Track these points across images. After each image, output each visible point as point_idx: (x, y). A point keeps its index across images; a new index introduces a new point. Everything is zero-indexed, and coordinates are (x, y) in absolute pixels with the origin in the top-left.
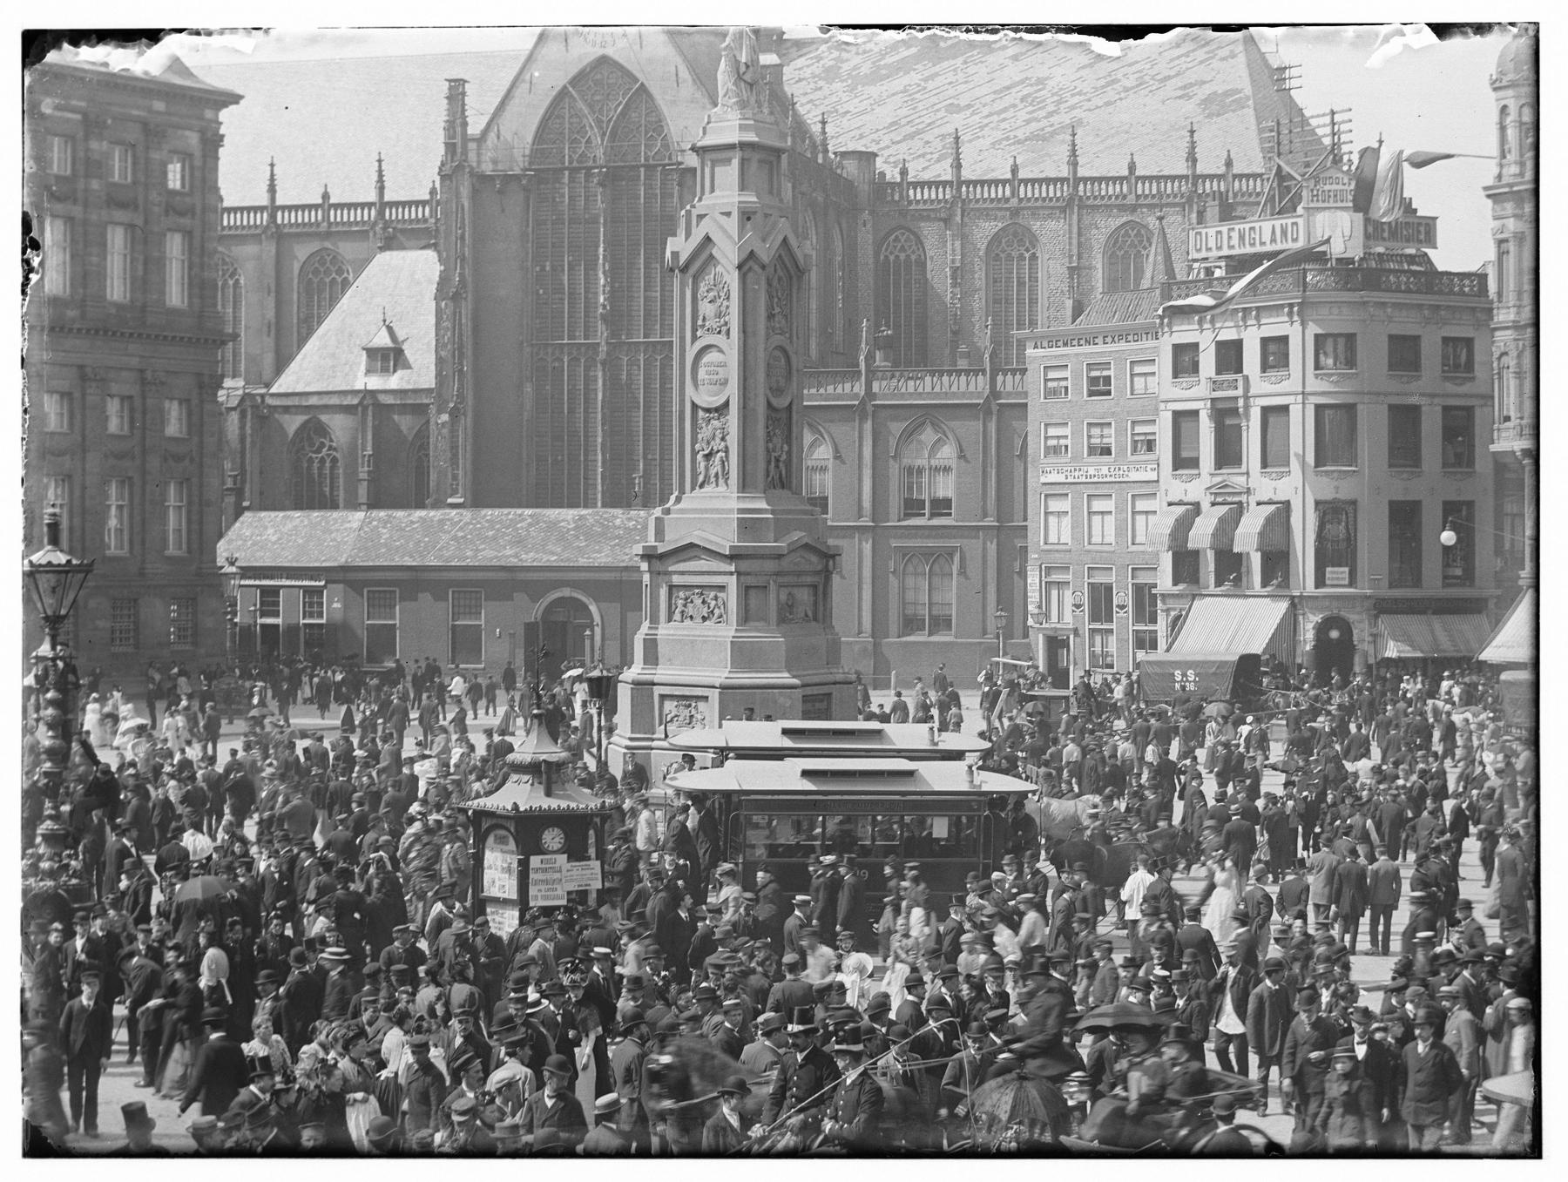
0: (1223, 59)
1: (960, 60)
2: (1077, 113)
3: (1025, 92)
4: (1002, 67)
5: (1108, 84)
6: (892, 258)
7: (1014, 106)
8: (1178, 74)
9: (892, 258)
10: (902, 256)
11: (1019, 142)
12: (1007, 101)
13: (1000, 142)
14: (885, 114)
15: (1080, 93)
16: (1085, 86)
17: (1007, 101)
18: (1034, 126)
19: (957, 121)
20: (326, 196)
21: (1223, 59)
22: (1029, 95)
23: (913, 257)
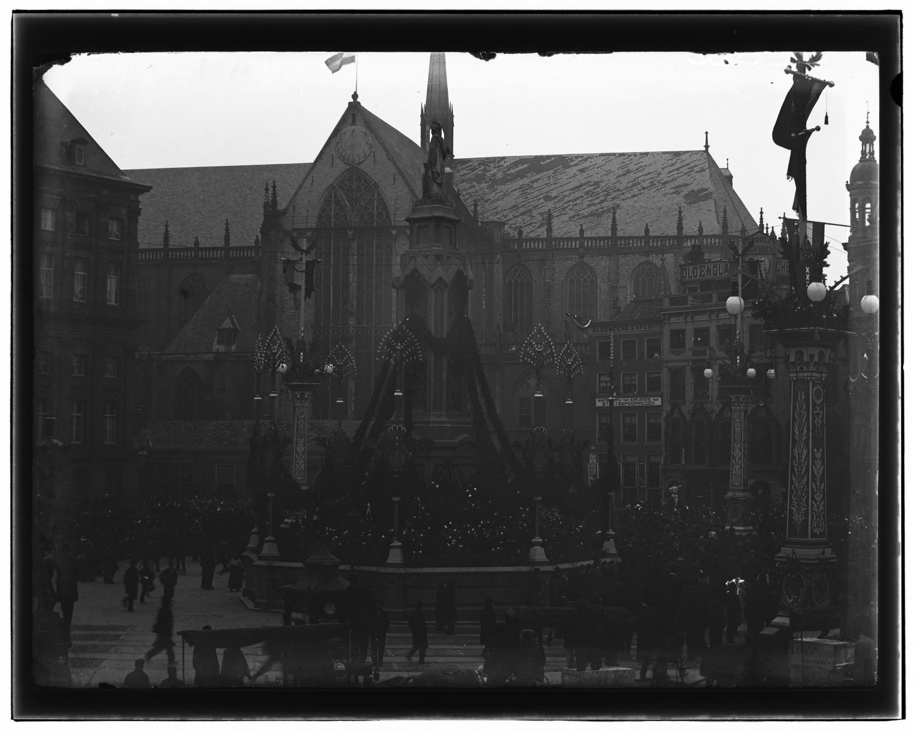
0: (696, 172)
1: (552, 171)
2: (618, 201)
3: (587, 190)
5: (635, 185)
6: (513, 281)
7: (582, 197)
9: (513, 281)
10: (519, 280)
11: (585, 217)
12: (577, 194)
13: (574, 217)
14: (509, 202)
16: (621, 187)
17: (577, 194)
18: (593, 208)
19: (550, 205)
20: (197, 243)
21: (696, 172)
22: (590, 191)
23: (525, 281)
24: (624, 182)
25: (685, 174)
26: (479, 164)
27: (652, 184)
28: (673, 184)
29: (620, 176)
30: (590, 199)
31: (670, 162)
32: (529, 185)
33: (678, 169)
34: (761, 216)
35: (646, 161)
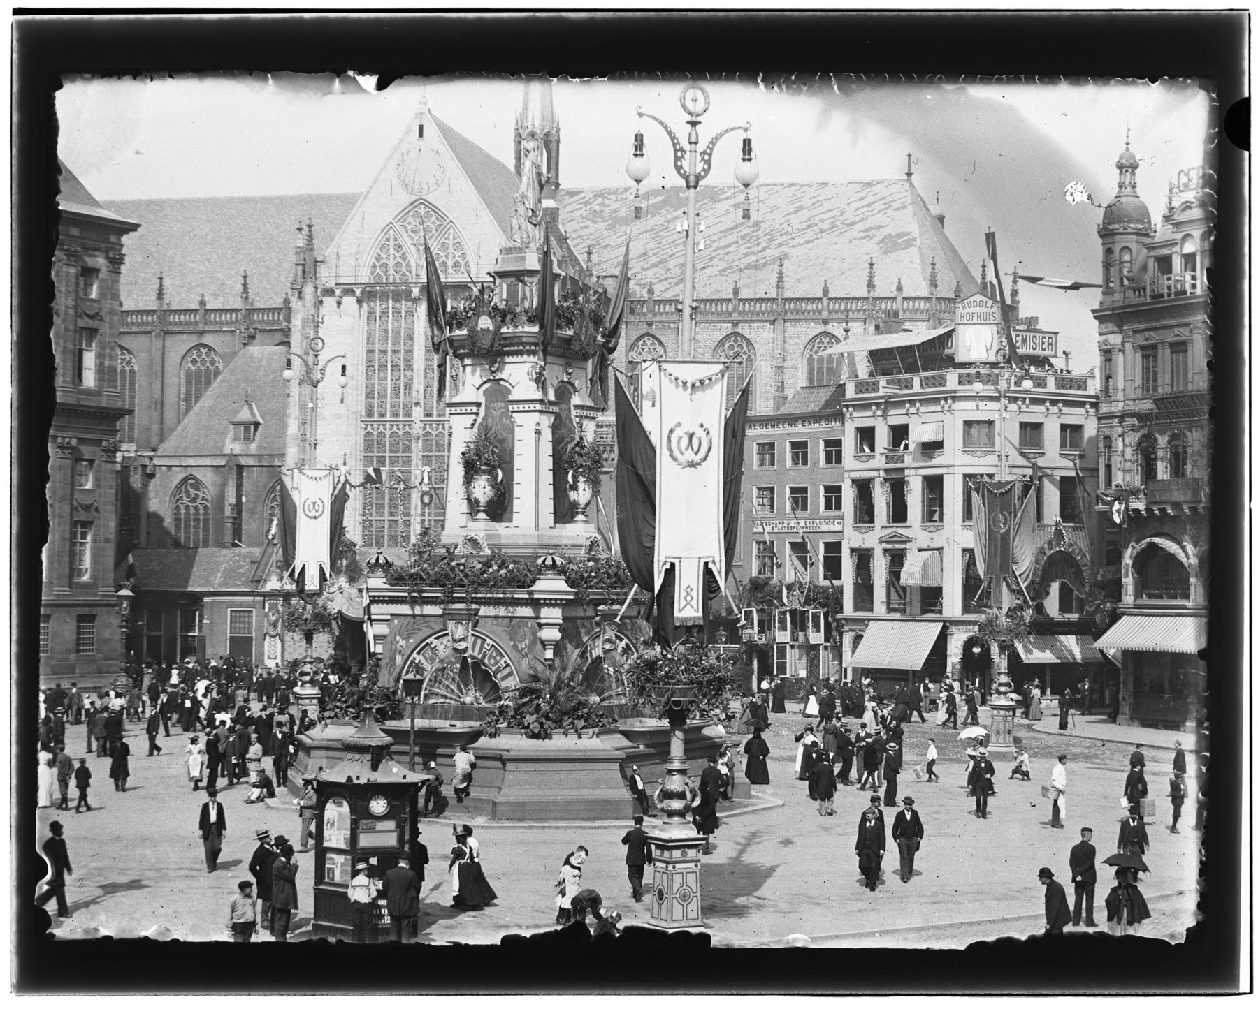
0: (897, 209)
2: (785, 249)
3: (744, 232)
4: (728, 212)
5: (809, 227)
7: (736, 243)
8: (862, 220)
12: (732, 238)
13: (725, 270)
15: (787, 233)
17: (732, 238)
18: (752, 258)
20: (203, 303)
21: (897, 209)
22: (747, 235)
24: (796, 221)
25: (879, 212)
26: (595, 196)
27: (834, 226)
28: (860, 226)
29: (791, 213)
30: (748, 245)
31: (859, 195)
32: (663, 225)
33: (868, 205)
34: (984, 271)
35: (824, 193)
